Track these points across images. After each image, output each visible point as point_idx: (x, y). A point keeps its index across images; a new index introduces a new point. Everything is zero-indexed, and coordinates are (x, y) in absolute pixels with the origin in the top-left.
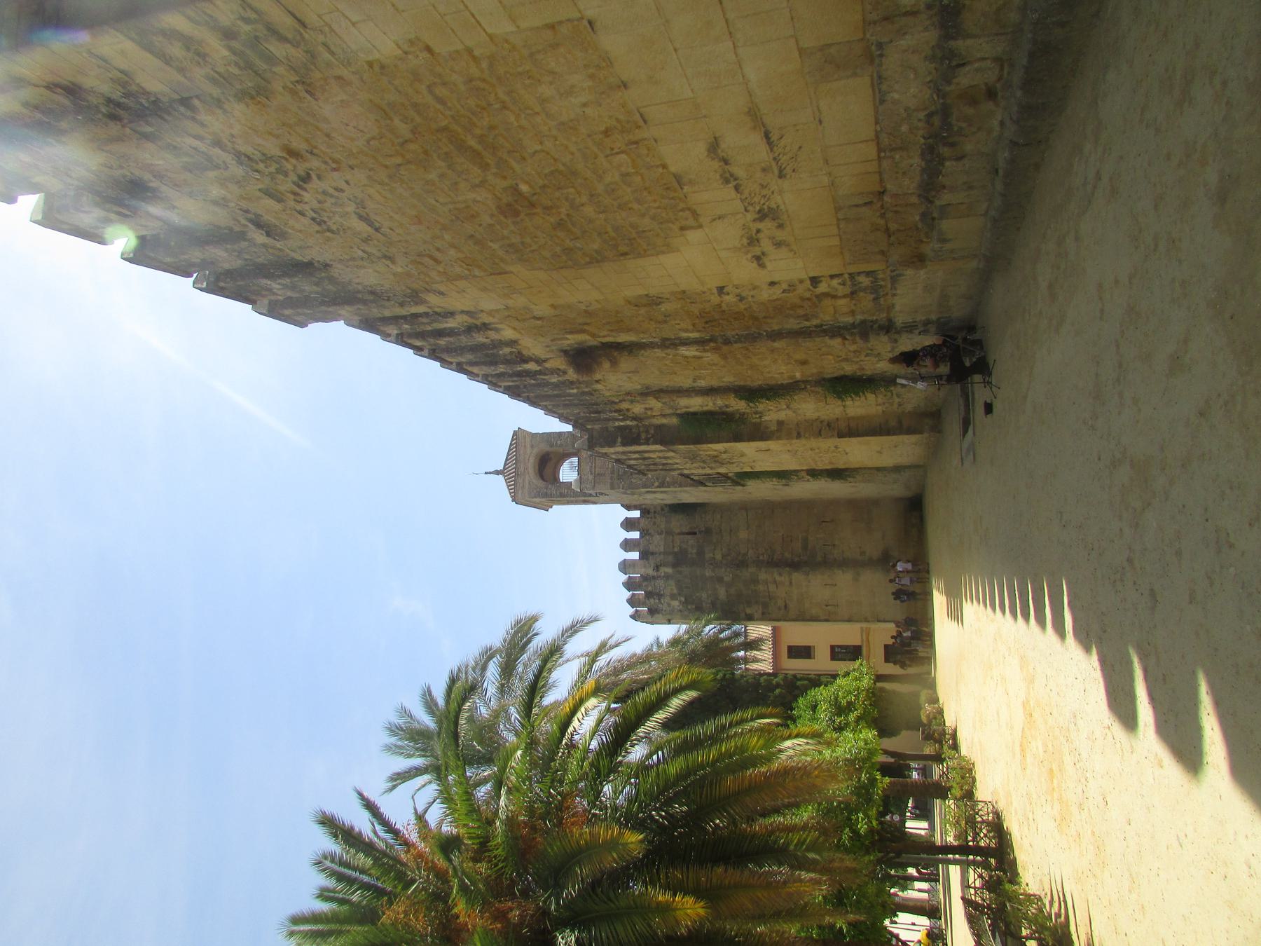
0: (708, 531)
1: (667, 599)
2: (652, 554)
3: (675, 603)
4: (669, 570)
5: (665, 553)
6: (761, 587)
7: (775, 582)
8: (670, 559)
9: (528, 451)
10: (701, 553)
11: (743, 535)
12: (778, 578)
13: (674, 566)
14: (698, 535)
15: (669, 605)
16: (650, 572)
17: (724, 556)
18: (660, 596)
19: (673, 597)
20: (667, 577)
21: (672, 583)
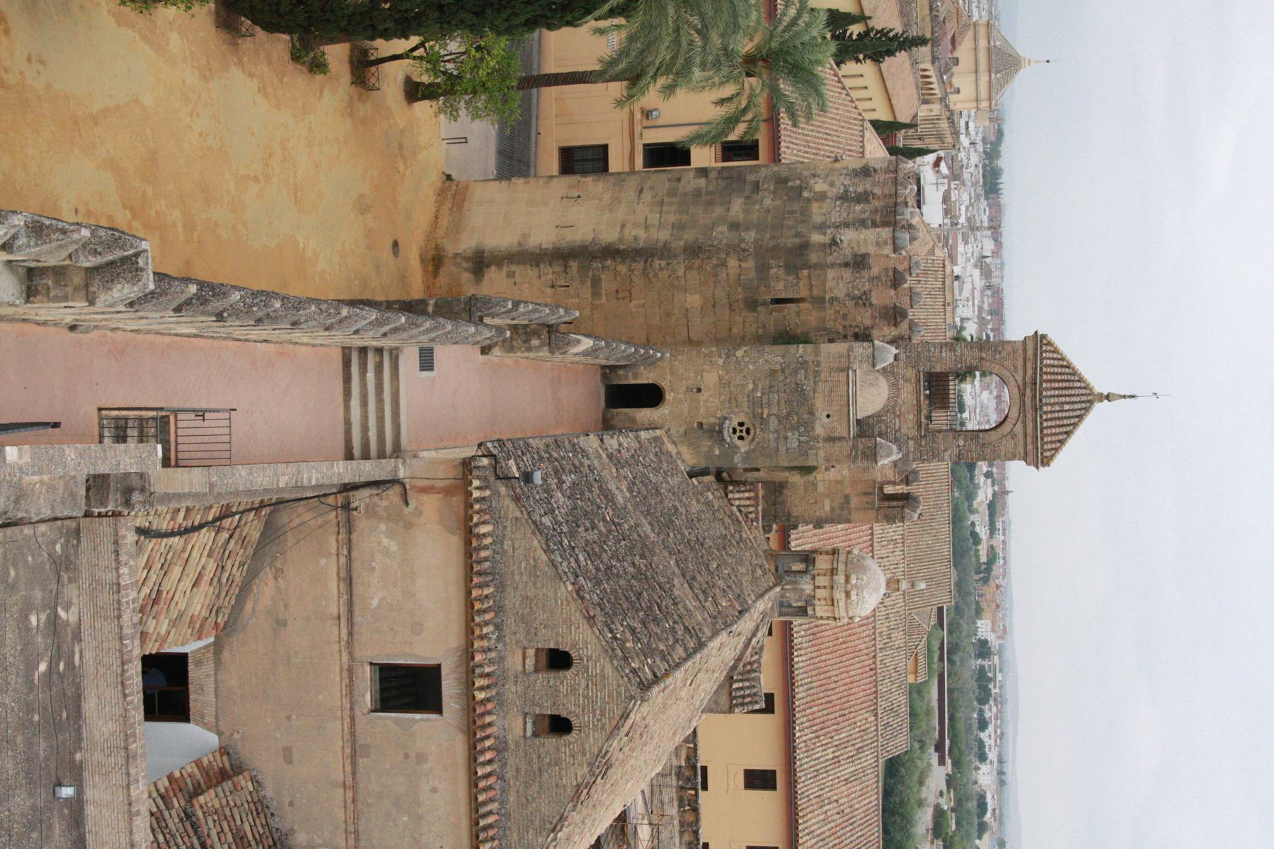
0: (752, 305)
1: (832, 192)
2: (847, 265)
3: (820, 186)
4: (816, 238)
5: (822, 266)
6: (671, 218)
7: (646, 227)
8: (814, 258)
9: (1019, 426)
10: (763, 268)
11: (694, 300)
12: (641, 233)
13: (805, 246)
14: (768, 298)
15: (832, 184)
16: (847, 236)
17: (724, 264)
18: (844, 197)
19: (822, 197)
20: (822, 228)
21: (817, 219)
